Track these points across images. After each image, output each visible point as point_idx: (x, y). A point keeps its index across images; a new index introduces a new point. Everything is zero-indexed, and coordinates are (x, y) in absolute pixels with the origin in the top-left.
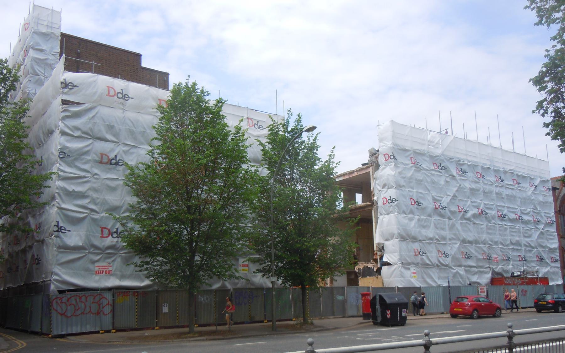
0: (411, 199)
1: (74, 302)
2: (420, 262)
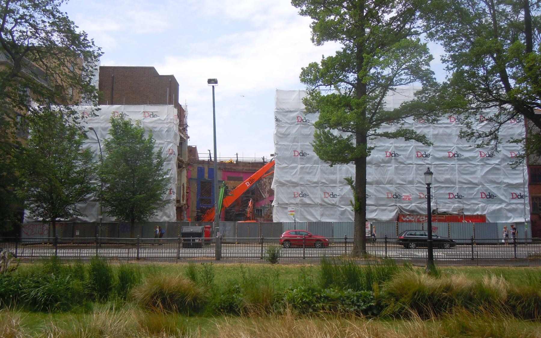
0: (295, 151)
1: (31, 228)
2: (300, 202)
